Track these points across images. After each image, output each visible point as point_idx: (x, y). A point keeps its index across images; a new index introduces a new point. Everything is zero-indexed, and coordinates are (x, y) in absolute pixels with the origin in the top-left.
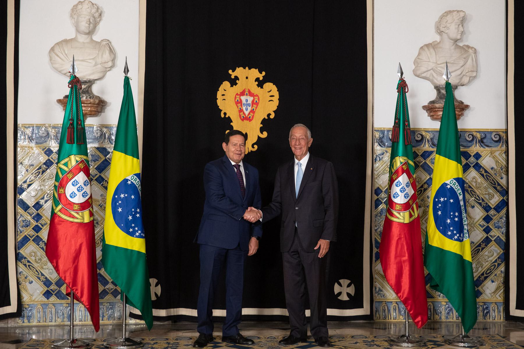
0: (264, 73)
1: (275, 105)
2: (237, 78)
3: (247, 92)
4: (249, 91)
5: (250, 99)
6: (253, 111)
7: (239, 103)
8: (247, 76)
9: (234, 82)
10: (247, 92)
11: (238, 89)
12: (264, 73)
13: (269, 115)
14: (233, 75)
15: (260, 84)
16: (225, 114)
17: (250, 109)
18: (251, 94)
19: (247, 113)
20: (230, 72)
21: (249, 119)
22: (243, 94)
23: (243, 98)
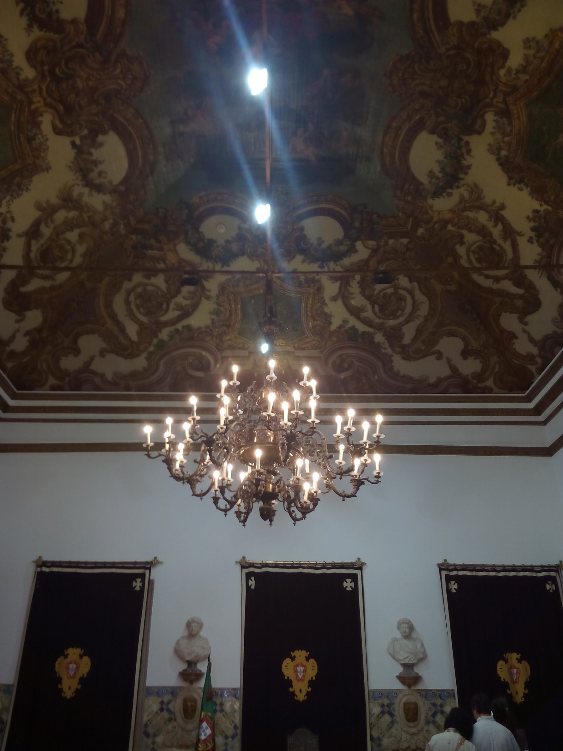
0: (309, 653)
1: (316, 671)
2: (295, 657)
3: (300, 664)
4: (302, 664)
5: (302, 669)
6: (304, 676)
7: (296, 671)
8: (300, 655)
9: (293, 659)
10: (300, 664)
11: (295, 663)
12: (309, 653)
13: (312, 678)
14: (293, 654)
15: (307, 659)
16: (288, 678)
17: (302, 674)
18: (303, 666)
19: (300, 677)
20: (292, 653)
21: (302, 680)
22: (298, 665)
23: (298, 668)
